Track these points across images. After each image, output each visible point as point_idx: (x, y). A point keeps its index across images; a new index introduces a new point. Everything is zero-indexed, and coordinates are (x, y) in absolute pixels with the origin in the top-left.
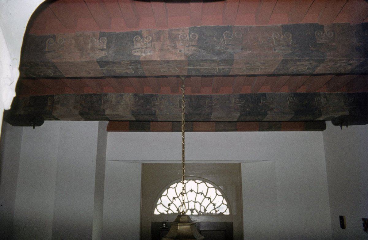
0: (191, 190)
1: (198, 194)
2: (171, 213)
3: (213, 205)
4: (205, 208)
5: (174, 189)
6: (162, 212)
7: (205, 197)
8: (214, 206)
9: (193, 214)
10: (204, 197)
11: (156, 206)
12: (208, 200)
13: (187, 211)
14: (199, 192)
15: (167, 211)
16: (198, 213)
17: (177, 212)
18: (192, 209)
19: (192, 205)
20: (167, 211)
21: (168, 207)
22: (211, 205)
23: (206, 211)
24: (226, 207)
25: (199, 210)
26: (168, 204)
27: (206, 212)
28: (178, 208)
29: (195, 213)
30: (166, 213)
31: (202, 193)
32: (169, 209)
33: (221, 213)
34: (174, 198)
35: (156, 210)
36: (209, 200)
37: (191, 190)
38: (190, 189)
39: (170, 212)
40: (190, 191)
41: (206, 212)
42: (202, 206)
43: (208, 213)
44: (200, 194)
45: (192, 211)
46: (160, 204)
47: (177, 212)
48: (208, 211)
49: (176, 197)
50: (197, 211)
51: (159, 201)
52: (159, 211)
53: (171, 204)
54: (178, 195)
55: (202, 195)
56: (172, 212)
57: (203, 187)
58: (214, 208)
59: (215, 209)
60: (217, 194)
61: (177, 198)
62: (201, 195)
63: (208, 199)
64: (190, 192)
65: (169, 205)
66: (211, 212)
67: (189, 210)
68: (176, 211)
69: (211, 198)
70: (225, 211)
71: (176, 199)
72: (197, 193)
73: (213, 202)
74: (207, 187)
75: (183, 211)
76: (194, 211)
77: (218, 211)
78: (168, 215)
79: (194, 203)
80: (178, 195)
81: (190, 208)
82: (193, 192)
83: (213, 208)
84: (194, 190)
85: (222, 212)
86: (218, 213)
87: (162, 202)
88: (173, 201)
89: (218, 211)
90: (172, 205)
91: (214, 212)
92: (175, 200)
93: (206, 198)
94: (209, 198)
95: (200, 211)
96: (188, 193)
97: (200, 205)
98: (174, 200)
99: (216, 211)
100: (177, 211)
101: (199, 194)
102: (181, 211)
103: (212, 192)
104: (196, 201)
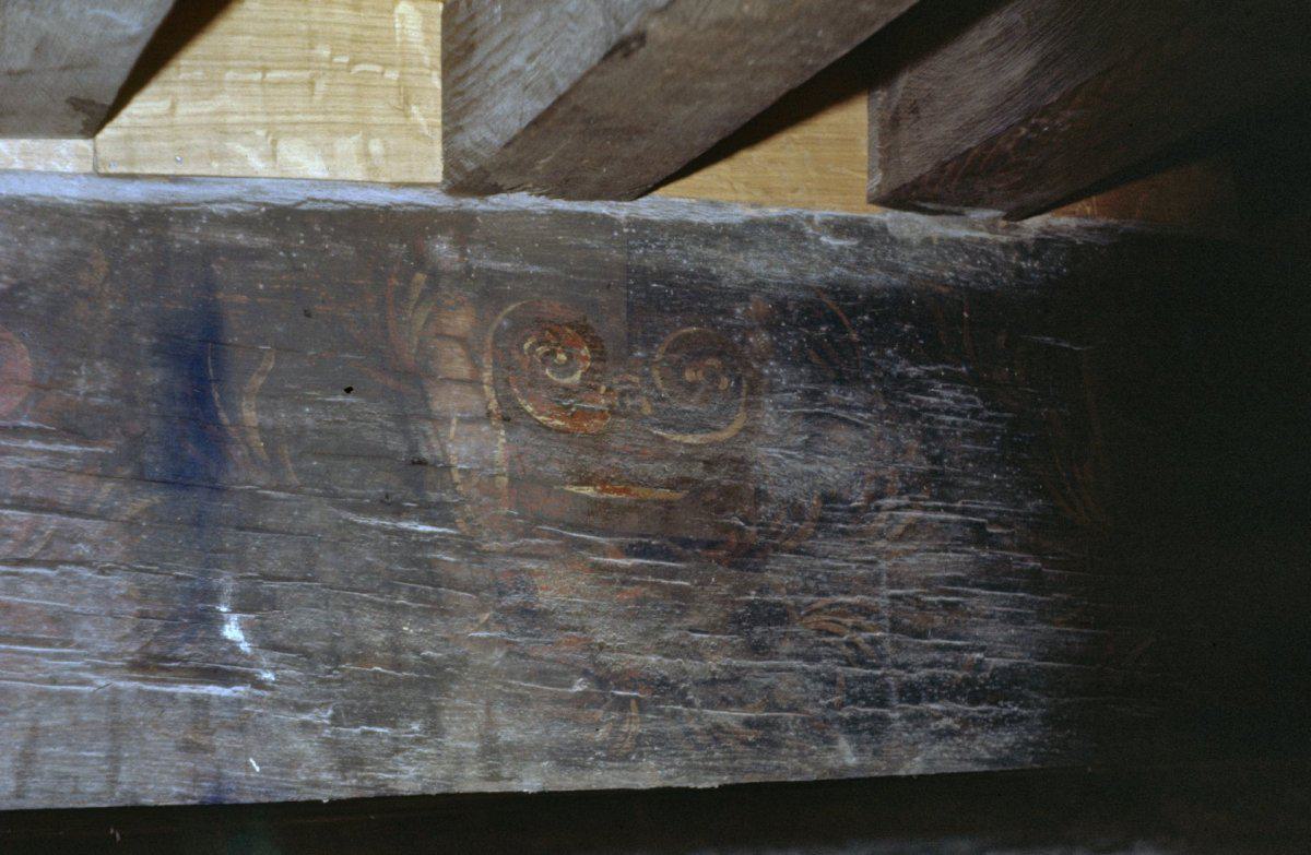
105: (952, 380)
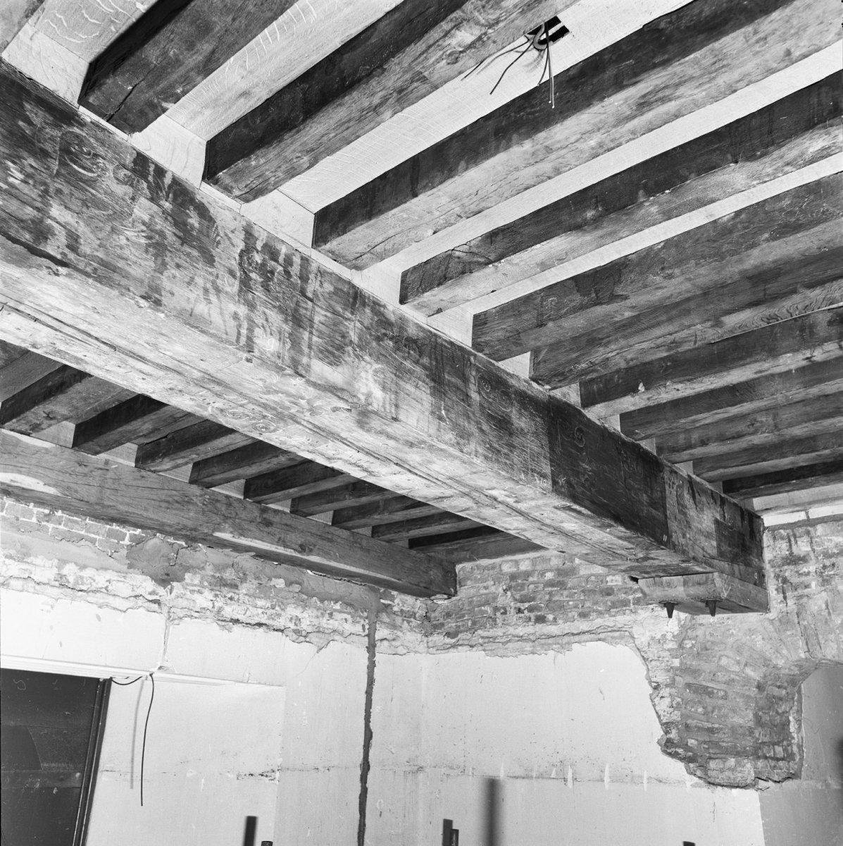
105: (539, 417)
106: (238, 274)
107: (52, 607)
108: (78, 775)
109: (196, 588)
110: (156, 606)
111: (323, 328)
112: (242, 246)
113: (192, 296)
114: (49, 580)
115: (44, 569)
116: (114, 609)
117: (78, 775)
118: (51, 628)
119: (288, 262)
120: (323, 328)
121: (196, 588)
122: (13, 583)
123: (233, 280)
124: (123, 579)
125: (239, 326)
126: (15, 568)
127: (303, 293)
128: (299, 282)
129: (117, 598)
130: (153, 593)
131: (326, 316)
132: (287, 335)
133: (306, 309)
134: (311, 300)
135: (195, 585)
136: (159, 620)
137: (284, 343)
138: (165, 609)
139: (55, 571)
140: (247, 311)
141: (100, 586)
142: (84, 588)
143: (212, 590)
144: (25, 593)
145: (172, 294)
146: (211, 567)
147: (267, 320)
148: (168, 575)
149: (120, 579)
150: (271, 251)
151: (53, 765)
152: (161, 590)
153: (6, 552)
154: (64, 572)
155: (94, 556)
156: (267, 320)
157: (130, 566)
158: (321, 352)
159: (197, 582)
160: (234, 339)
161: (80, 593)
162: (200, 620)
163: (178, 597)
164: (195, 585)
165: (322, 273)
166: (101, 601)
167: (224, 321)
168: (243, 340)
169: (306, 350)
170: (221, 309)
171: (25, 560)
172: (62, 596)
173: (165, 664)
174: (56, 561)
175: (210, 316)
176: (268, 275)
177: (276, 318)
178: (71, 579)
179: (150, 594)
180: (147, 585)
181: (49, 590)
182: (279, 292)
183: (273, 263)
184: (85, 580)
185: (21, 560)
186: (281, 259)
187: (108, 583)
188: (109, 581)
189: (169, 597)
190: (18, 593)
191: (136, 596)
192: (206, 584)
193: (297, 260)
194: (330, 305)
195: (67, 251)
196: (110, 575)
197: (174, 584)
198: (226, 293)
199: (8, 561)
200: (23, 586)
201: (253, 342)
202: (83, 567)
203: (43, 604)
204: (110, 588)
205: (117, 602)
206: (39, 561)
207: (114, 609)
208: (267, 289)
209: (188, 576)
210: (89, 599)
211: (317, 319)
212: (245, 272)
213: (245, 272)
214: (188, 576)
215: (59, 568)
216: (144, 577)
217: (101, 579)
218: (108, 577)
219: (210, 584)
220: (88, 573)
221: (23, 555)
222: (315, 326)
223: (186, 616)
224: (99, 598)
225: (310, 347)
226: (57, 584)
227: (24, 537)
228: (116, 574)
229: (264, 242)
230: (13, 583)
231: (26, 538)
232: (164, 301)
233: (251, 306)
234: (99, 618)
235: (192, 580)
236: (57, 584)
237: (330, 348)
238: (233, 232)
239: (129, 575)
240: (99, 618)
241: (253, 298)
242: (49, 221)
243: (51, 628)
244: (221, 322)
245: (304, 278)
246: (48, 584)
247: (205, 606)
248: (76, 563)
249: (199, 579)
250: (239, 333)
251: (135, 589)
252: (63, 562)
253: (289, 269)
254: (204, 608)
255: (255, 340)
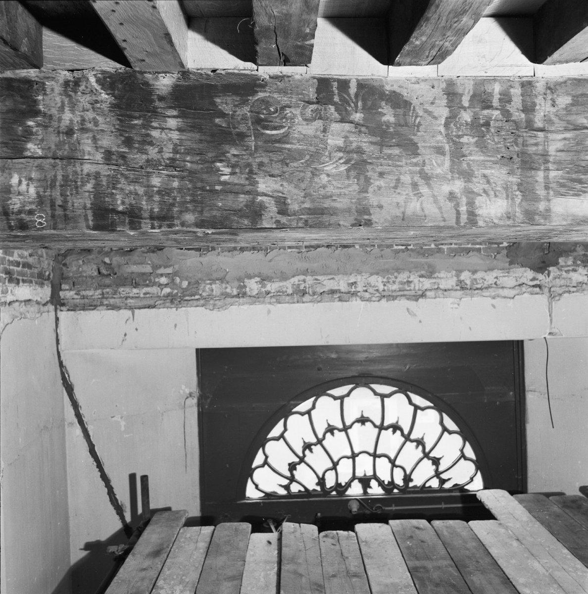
0: (362, 416)
1: (383, 432)
2: (300, 491)
3: (430, 462)
4: (408, 472)
5: (307, 416)
6: (269, 489)
7: (407, 438)
8: (434, 467)
9: (369, 491)
10: (403, 439)
11: (249, 473)
12: (417, 447)
13: (348, 485)
14: (386, 424)
15: (287, 487)
16: (384, 488)
17: (318, 488)
18: (365, 475)
19: (364, 466)
20: (287, 487)
21: (288, 474)
22: (427, 463)
23: (411, 480)
24: (471, 467)
25: (386, 479)
26: (289, 464)
27: (411, 485)
28: (321, 476)
29: (375, 490)
30: (283, 492)
31: (396, 427)
32: (292, 479)
33: (456, 485)
34: (308, 446)
35: (250, 487)
36: (420, 448)
37: (362, 416)
38: (359, 416)
39: (295, 488)
40: (358, 421)
41: (411, 485)
42: (397, 467)
43: (415, 487)
44: (391, 429)
45: (365, 482)
46: (263, 466)
47: (318, 488)
48: (418, 480)
49: (314, 440)
50: (381, 483)
51: (259, 459)
52: (260, 487)
53: (299, 463)
54: (320, 436)
55: (398, 432)
56: (303, 489)
57: (398, 407)
58: (437, 470)
59: (437, 474)
60: (445, 429)
61: (315, 445)
62: (394, 432)
63: (415, 444)
64: (360, 424)
65: (292, 467)
66: (427, 485)
67: (356, 481)
68: (311, 483)
69: (425, 440)
70: (468, 479)
71: (313, 447)
72: (381, 428)
73: (432, 455)
74: (412, 408)
75: (338, 485)
76: (373, 483)
77: (449, 479)
78: (290, 495)
79: (372, 458)
80: (320, 436)
81: (359, 473)
82: (368, 424)
83: (433, 473)
84: (372, 418)
85: (461, 481)
86: (447, 486)
87: (269, 460)
88: (304, 456)
89: (449, 479)
90: (301, 468)
91: (435, 483)
92: (311, 451)
93: (408, 443)
94: (420, 442)
95: (392, 483)
96: (350, 427)
97: (390, 465)
98: (307, 452)
99: (443, 482)
100: (317, 484)
101: (387, 428)
102: (330, 482)
103: (429, 422)
104: (378, 452)
106: (447, 147)
107: (458, 305)
108: (511, 393)
109: (570, 268)
110: (537, 289)
111: (563, 156)
112: (444, 112)
113: (401, 199)
114: (452, 286)
115: (447, 280)
116: (505, 297)
117: (511, 393)
118: (461, 318)
119: (506, 98)
120: (563, 156)
121: (570, 268)
122: (428, 293)
123: (442, 158)
124: (507, 274)
125: (457, 205)
126: (427, 283)
127: (529, 126)
128: (523, 116)
129: (505, 290)
130: (534, 279)
131: (565, 139)
132: (516, 188)
133: (536, 144)
134: (542, 130)
135: (569, 266)
136: (542, 300)
137: (513, 199)
138: (546, 290)
139: (455, 279)
140: (463, 184)
141: (490, 282)
142: (479, 286)
143: (585, 266)
144: (438, 299)
145: (381, 207)
146: (582, 247)
147: (488, 182)
148: (544, 262)
149: (504, 275)
150: (482, 99)
151: (493, 388)
152: (540, 276)
153: (419, 273)
154: (462, 278)
155: (481, 262)
156: (488, 182)
157: (511, 263)
158: (562, 185)
159: (570, 262)
160: (452, 222)
161: (476, 291)
162: (578, 294)
163: (555, 278)
164: (569, 266)
165: (552, 88)
166: (493, 294)
167: (440, 208)
168: (464, 218)
169: (541, 192)
170: (434, 196)
171: (433, 276)
172: (464, 296)
173: (553, 331)
174: (454, 272)
175: (423, 210)
176: (480, 127)
177: (499, 174)
178: (468, 282)
179: (532, 280)
180: (529, 274)
181: (453, 293)
182: (499, 142)
183: (486, 112)
184: (478, 281)
185: (430, 277)
186: (495, 103)
187: (496, 280)
188: (496, 278)
189: (548, 280)
190: (433, 300)
191: (520, 285)
192: (579, 262)
193: (516, 92)
194: (568, 122)
195: (279, 217)
196: (495, 273)
197: (551, 269)
198: (437, 176)
199: (421, 279)
200: (435, 295)
201: (476, 216)
202: (474, 272)
203: (452, 303)
204: (498, 283)
205: (506, 292)
206: (442, 275)
207: (505, 297)
208: (482, 146)
209: (561, 261)
210: (484, 294)
211: (552, 149)
212: (455, 143)
213: (455, 143)
214: (561, 261)
215: (458, 276)
216: (524, 269)
217: (490, 278)
218: (495, 275)
219: (583, 262)
220: (479, 275)
221: (430, 273)
222: (551, 159)
223: (565, 292)
224: (491, 292)
225: (547, 188)
226: (458, 288)
227: (428, 260)
228: (501, 271)
229: (471, 93)
230: (428, 293)
231: (430, 260)
232: (374, 218)
233: (467, 175)
234: (494, 306)
235: (566, 262)
236: (458, 288)
237: (574, 176)
238: (432, 103)
239: (512, 270)
240: (494, 306)
241: (468, 165)
242: (260, 198)
243: (461, 318)
244: (437, 211)
245: (528, 109)
246: (452, 290)
247: (581, 280)
248: (469, 271)
249: (572, 260)
250: (458, 213)
251: (518, 279)
252: (459, 272)
253: (508, 107)
254: (580, 283)
255: (479, 212)
